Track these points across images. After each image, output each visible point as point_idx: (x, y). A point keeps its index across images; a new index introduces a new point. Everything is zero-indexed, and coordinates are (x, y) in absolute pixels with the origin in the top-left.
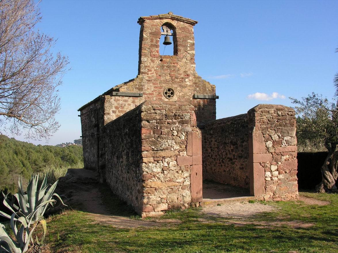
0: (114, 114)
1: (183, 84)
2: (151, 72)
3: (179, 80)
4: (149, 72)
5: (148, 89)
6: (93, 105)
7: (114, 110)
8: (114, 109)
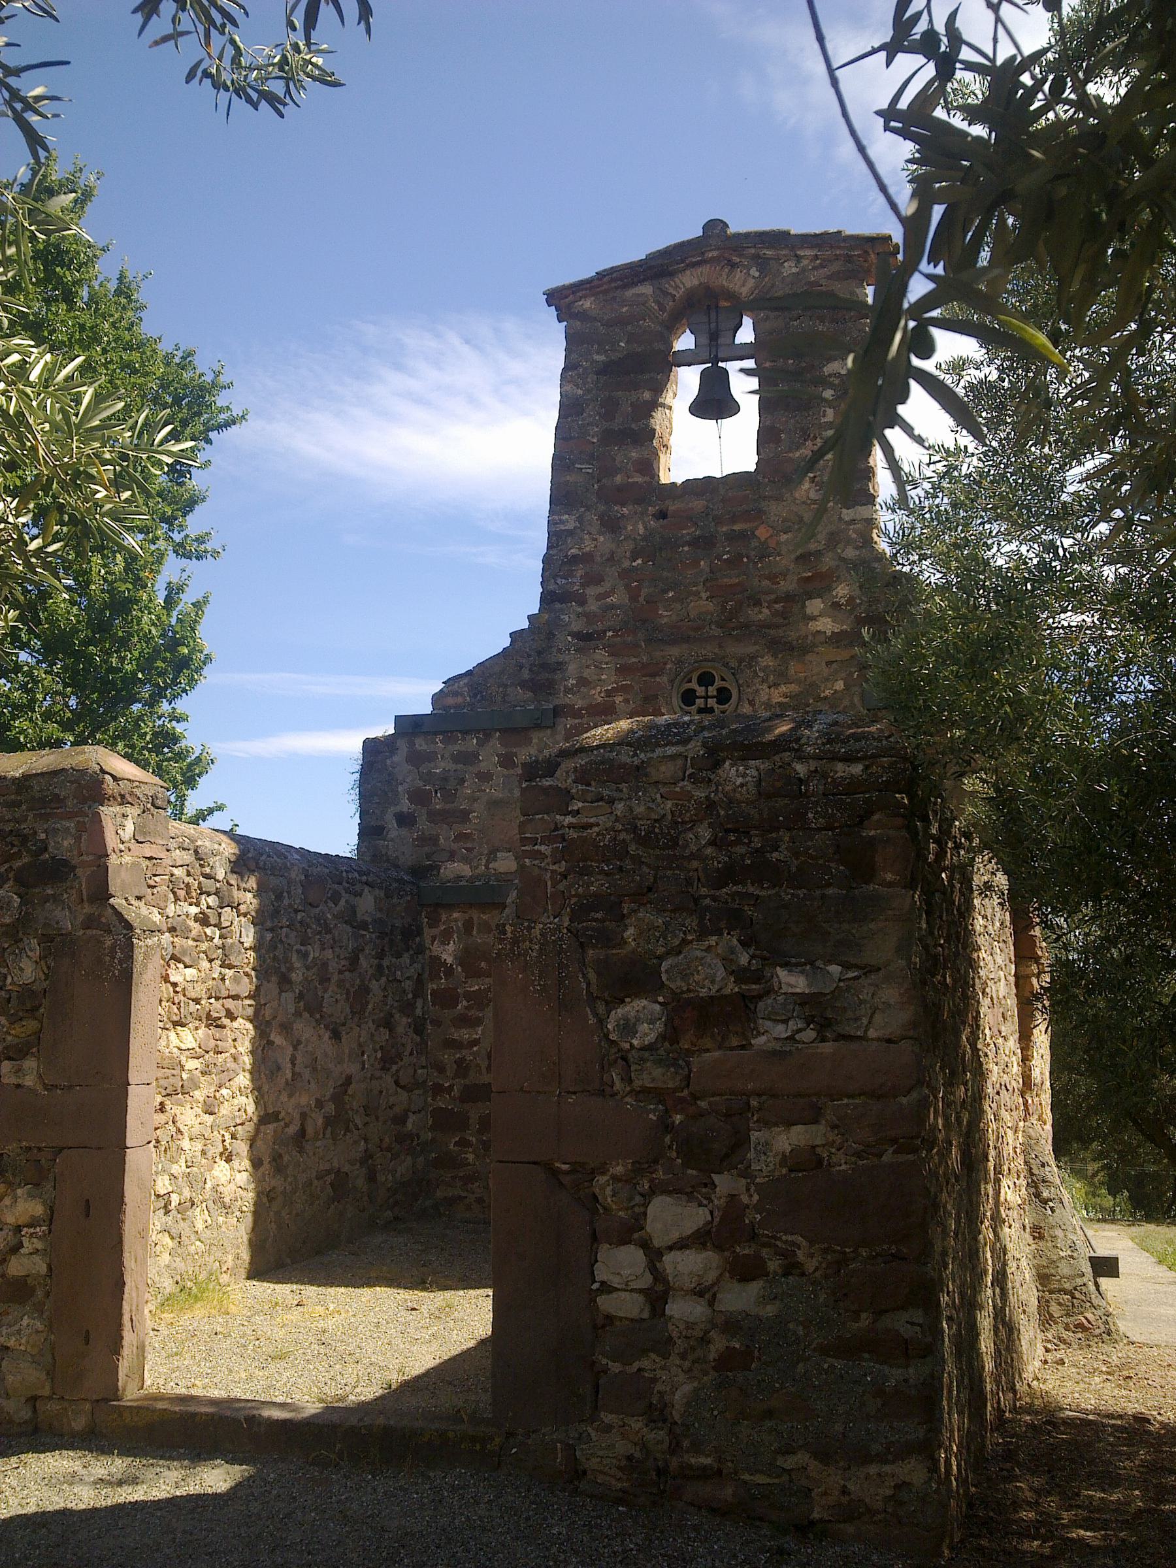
0: (404, 832)
1: (792, 635)
2: (600, 590)
3: (766, 611)
4: (592, 591)
5: (583, 682)
6: (979, 130)
7: (405, 809)
8: (405, 805)
